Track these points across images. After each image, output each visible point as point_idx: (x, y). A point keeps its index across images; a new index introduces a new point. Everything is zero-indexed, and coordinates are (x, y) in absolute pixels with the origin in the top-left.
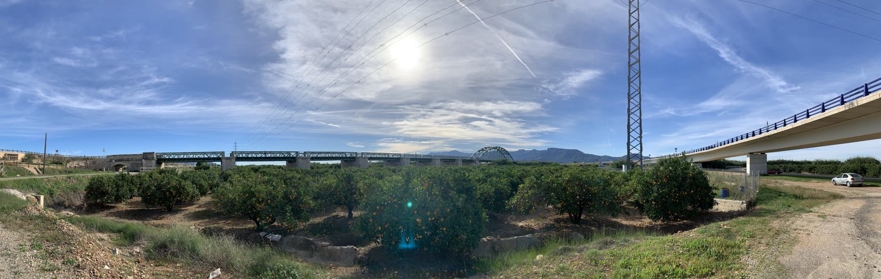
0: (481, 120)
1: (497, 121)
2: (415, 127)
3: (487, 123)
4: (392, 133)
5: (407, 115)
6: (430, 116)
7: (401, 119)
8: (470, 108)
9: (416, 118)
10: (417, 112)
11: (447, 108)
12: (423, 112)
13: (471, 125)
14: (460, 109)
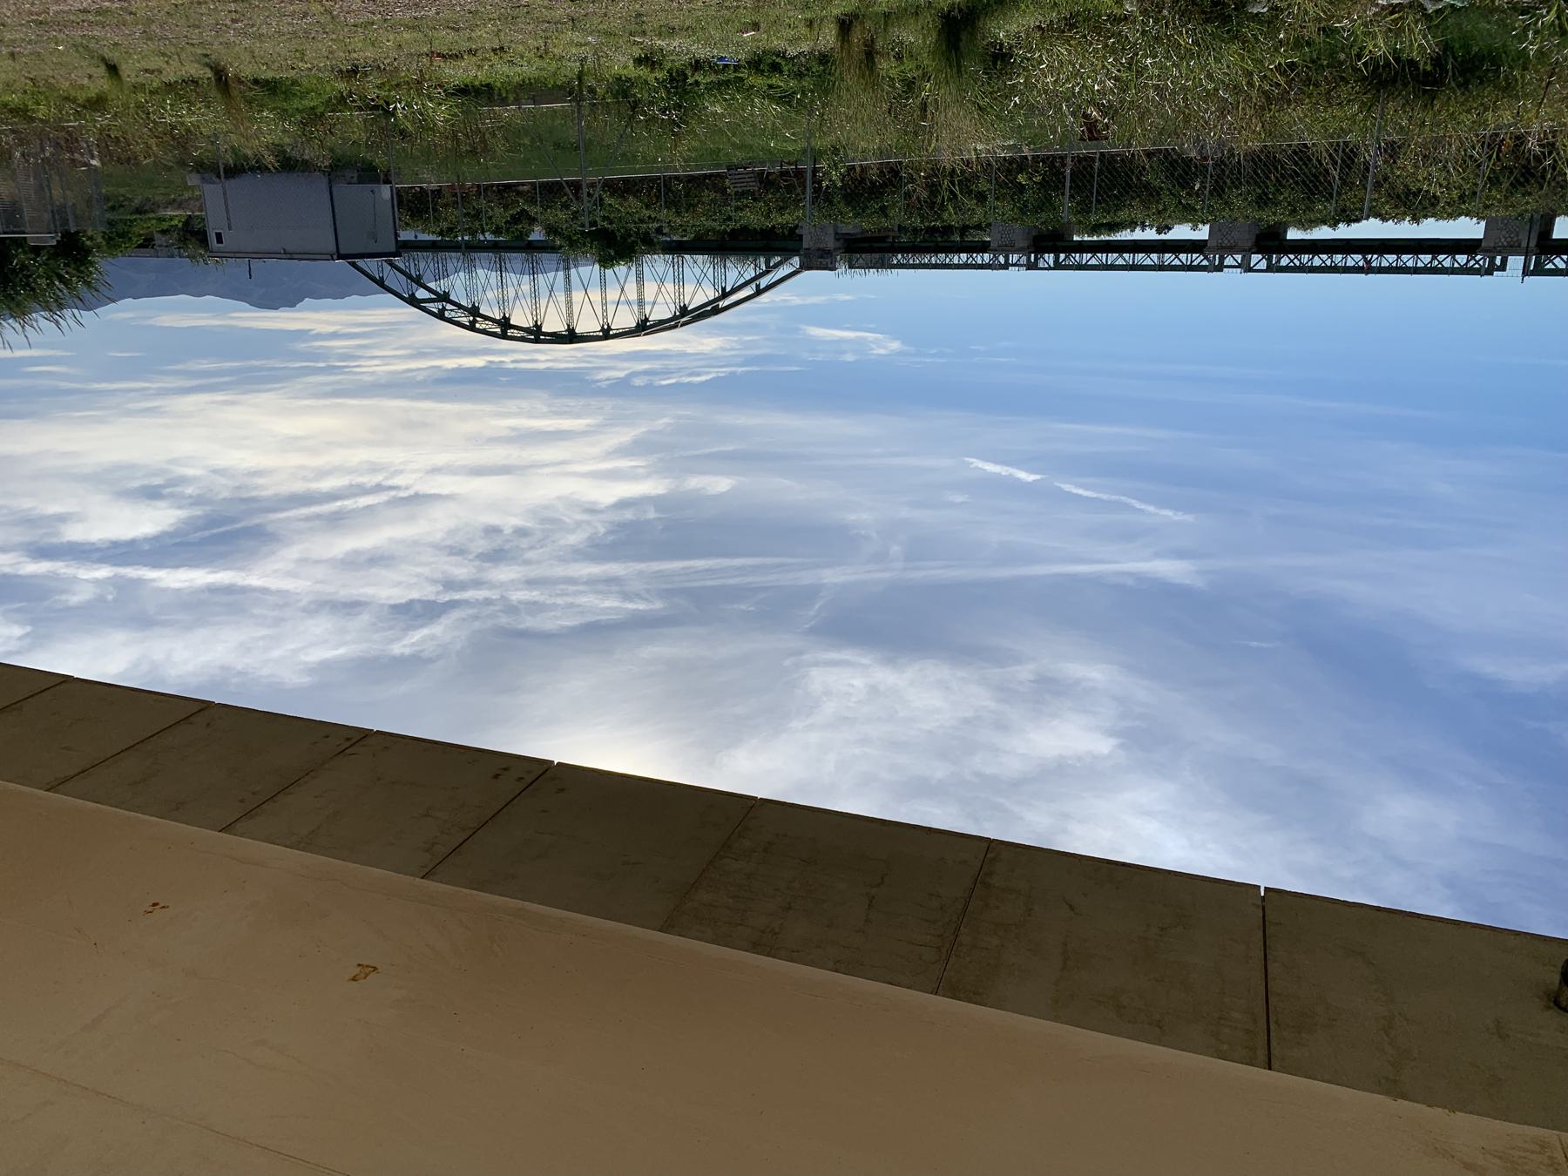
0: (115, 544)
2: (534, 466)
3: (74, 533)
5: (598, 550)
6: (457, 551)
7: (629, 515)
10: (535, 572)
12: (504, 574)
13: (178, 500)
14: (278, 622)
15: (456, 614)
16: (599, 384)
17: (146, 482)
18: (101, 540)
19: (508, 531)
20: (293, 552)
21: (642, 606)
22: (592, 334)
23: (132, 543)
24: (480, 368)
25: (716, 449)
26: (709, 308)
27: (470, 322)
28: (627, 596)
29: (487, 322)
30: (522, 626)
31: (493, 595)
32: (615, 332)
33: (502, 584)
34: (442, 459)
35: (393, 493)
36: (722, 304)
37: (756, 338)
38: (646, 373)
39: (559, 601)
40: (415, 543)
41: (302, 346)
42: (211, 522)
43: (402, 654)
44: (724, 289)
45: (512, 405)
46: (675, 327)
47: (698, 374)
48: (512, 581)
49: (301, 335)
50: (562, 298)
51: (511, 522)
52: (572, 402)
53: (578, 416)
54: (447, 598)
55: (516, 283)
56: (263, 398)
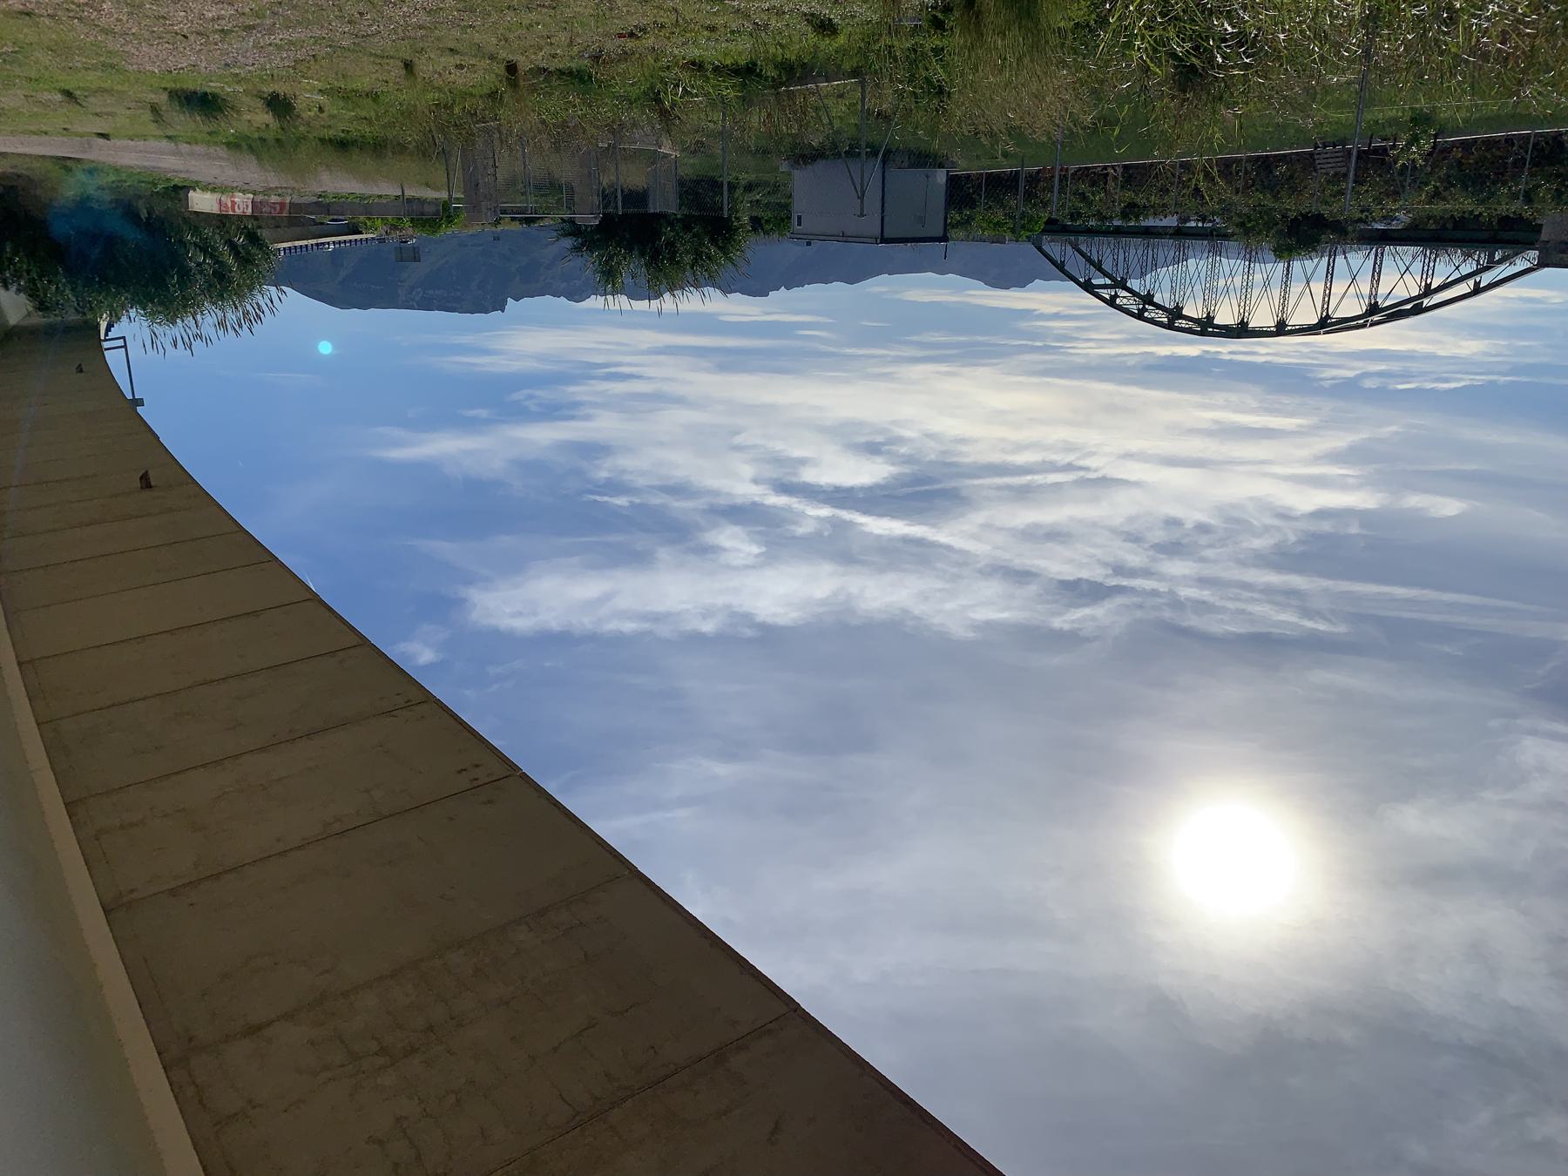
0: (838, 489)
1: (742, 484)
4: (1390, 427)
5: (1282, 559)
6: (1135, 538)
8: (891, 577)
9: (1234, 523)
10: (1209, 571)
11: (1033, 588)
12: (1178, 568)
13: (894, 458)
15: (1120, 600)
16: (1322, 383)
17: (869, 439)
18: (827, 484)
19: (1189, 525)
20: (979, 517)
21: (1322, 627)
22: (1265, 329)
23: (851, 490)
24: (1193, 357)
25: (1453, 466)
26: (1409, 306)
27: (1138, 309)
28: (1307, 613)
29: (1157, 311)
30: (1185, 624)
31: (1162, 587)
32: (1289, 328)
33: (1172, 579)
34: (1135, 445)
35: (1081, 473)
36: (1426, 302)
37: (1533, 343)
38: (1380, 374)
39: (1231, 605)
40: (1094, 525)
41: (1023, 325)
42: (917, 480)
43: (1061, 629)
44: (1428, 286)
45: (1220, 398)
46: (1363, 326)
47: (1447, 380)
48: (1184, 576)
49: (1026, 314)
50: (1276, 293)
51: (1192, 516)
52: (1285, 400)
53: (1291, 414)
54: (1113, 582)
55: (1227, 270)
56: (983, 372)
